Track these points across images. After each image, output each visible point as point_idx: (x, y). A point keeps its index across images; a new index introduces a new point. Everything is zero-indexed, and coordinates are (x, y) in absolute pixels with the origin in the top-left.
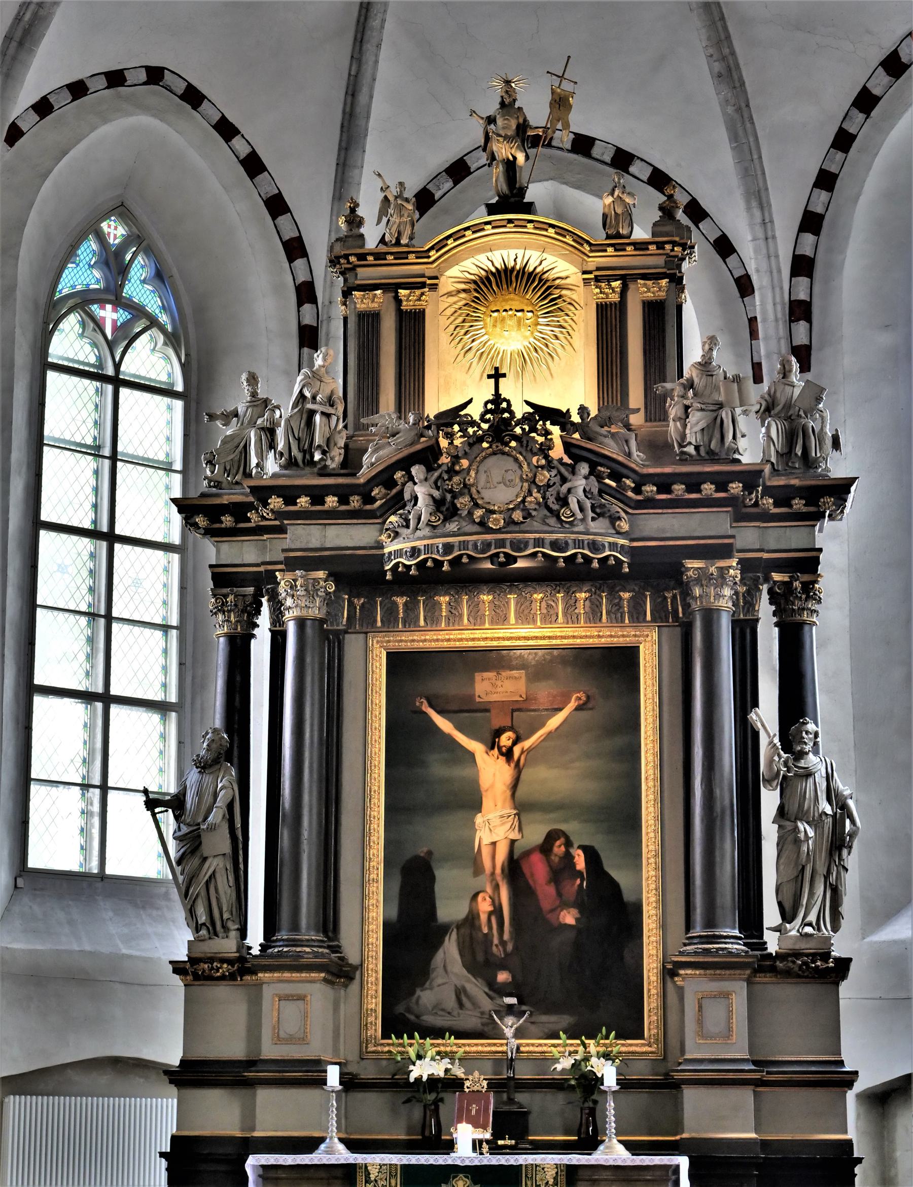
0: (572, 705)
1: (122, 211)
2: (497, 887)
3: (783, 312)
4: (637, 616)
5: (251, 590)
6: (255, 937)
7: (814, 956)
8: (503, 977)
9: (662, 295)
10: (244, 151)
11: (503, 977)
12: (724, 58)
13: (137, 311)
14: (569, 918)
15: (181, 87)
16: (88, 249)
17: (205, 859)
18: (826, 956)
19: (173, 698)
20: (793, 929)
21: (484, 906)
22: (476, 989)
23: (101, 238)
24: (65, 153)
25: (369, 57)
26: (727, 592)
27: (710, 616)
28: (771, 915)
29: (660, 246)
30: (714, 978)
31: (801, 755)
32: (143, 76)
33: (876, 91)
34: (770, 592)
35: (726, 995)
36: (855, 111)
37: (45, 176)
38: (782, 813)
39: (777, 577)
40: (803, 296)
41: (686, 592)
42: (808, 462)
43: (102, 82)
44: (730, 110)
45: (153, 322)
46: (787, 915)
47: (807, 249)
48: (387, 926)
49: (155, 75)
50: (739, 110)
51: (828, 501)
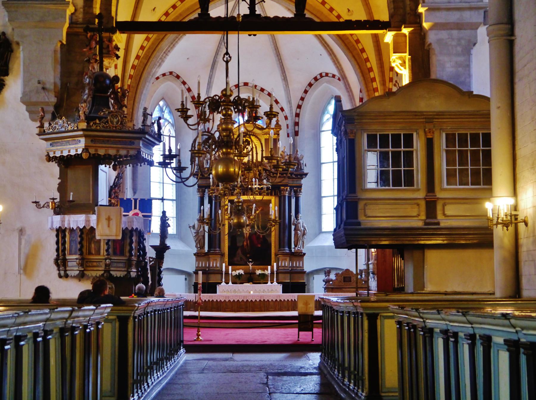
0: (260, 210)
1: (163, 99)
2: (247, 241)
3: (293, 124)
4: (271, 195)
5: (204, 189)
6: (206, 249)
7: (300, 253)
8: (248, 255)
9: (276, 137)
10: (187, 87)
11: (248, 255)
12: (284, 76)
13: (166, 120)
14: (259, 246)
15: (176, 75)
16: (157, 108)
17: (199, 236)
18: (302, 253)
19: (175, 198)
20: (296, 248)
21: (245, 244)
22: (244, 258)
23: (159, 105)
24: (155, 92)
25: (214, 72)
26: (287, 192)
27: (285, 196)
28: (293, 246)
29: (276, 129)
30: (284, 256)
31: (298, 220)
32: (169, 74)
33: (312, 83)
34: (294, 190)
35: (286, 259)
36: (308, 87)
37: (152, 97)
38: (295, 229)
39: (295, 189)
40: (297, 121)
41: (280, 192)
42: (301, 169)
43: (162, 76)
44: (285, 86)
45: (169, 122)
46: (296, 246)
47: (298, 112)
48: (229, 247)
49: (171, 73)
50: (286, 86)
51: (304, 176)
